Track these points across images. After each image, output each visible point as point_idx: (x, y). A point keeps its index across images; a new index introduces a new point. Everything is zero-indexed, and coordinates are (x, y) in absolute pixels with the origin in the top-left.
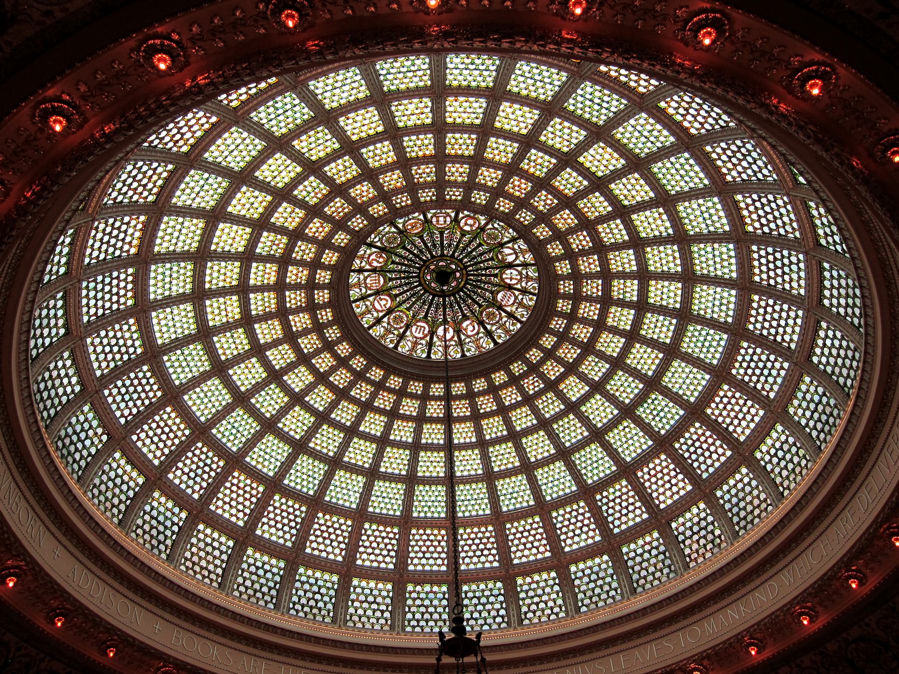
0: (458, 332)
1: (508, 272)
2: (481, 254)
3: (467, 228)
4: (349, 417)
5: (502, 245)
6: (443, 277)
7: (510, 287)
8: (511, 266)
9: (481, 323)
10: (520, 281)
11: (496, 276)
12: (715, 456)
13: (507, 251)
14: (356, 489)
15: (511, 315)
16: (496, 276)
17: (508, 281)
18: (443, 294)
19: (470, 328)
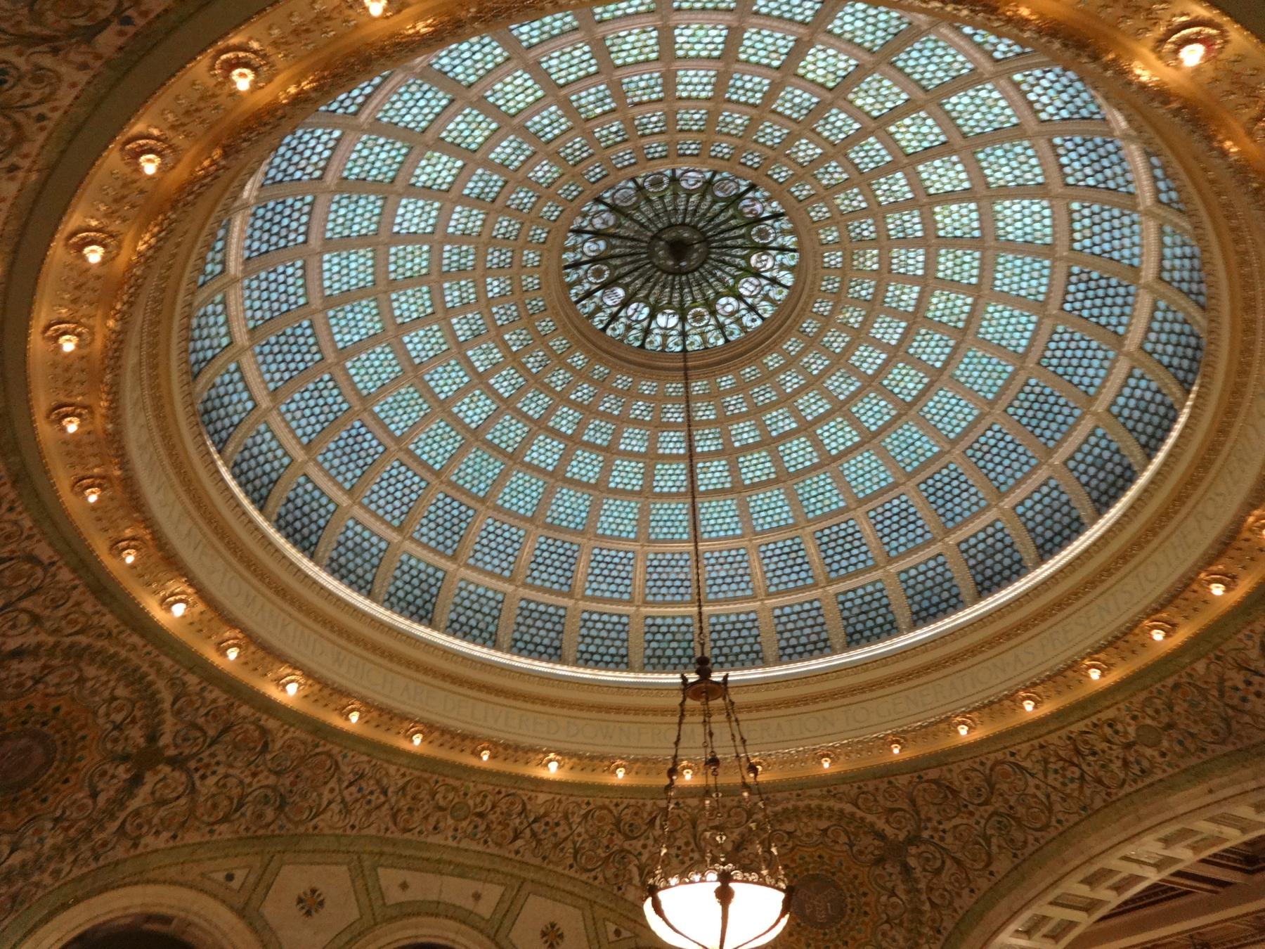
0: (597, 234)
1: (646, 311)
2: (682, 295)
3: (723, 301)
4: (583, 102)
5: (683, 319)
6: (679, 249)
7: (625, 304)
8: (652, 316)
9: (594, 261)
10: (629, 318)
11: (647, 297)
12: (389, 508)
13: (673, 321)
14: (459, 69)
15: (589, 294)
16: (647, 297)
17: (634, 306)
18: (656, 237)
19: (594, 247)
